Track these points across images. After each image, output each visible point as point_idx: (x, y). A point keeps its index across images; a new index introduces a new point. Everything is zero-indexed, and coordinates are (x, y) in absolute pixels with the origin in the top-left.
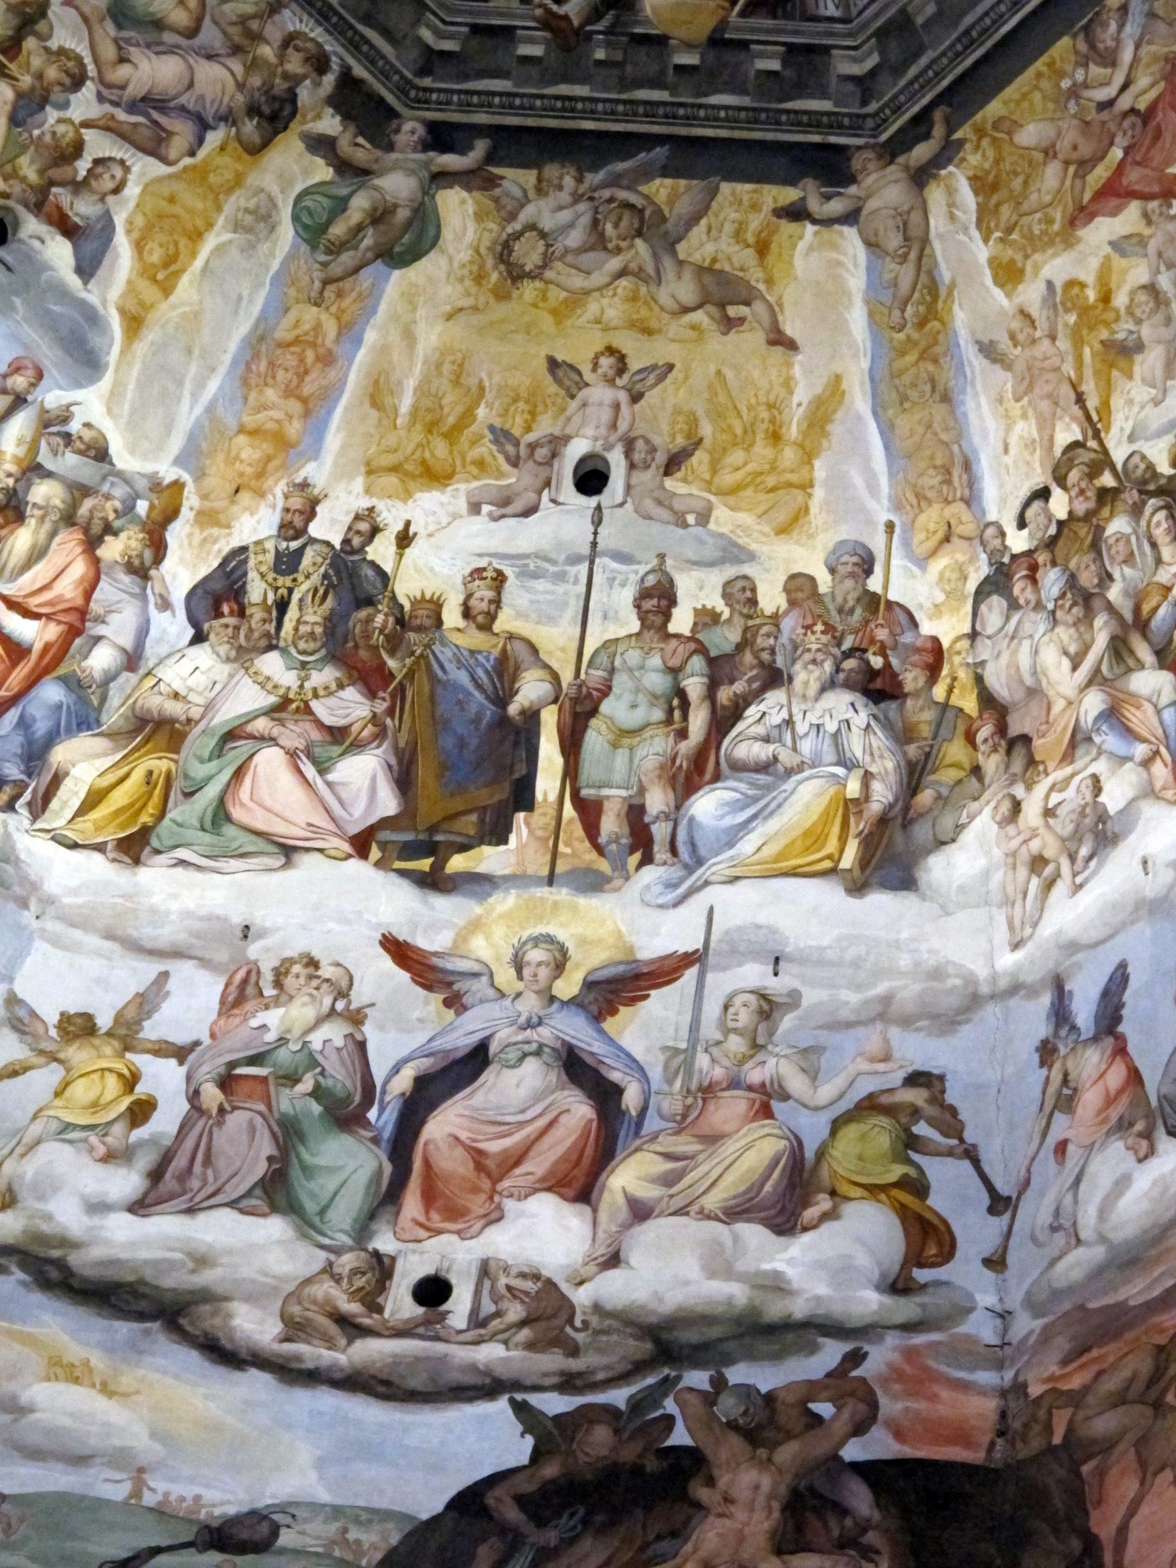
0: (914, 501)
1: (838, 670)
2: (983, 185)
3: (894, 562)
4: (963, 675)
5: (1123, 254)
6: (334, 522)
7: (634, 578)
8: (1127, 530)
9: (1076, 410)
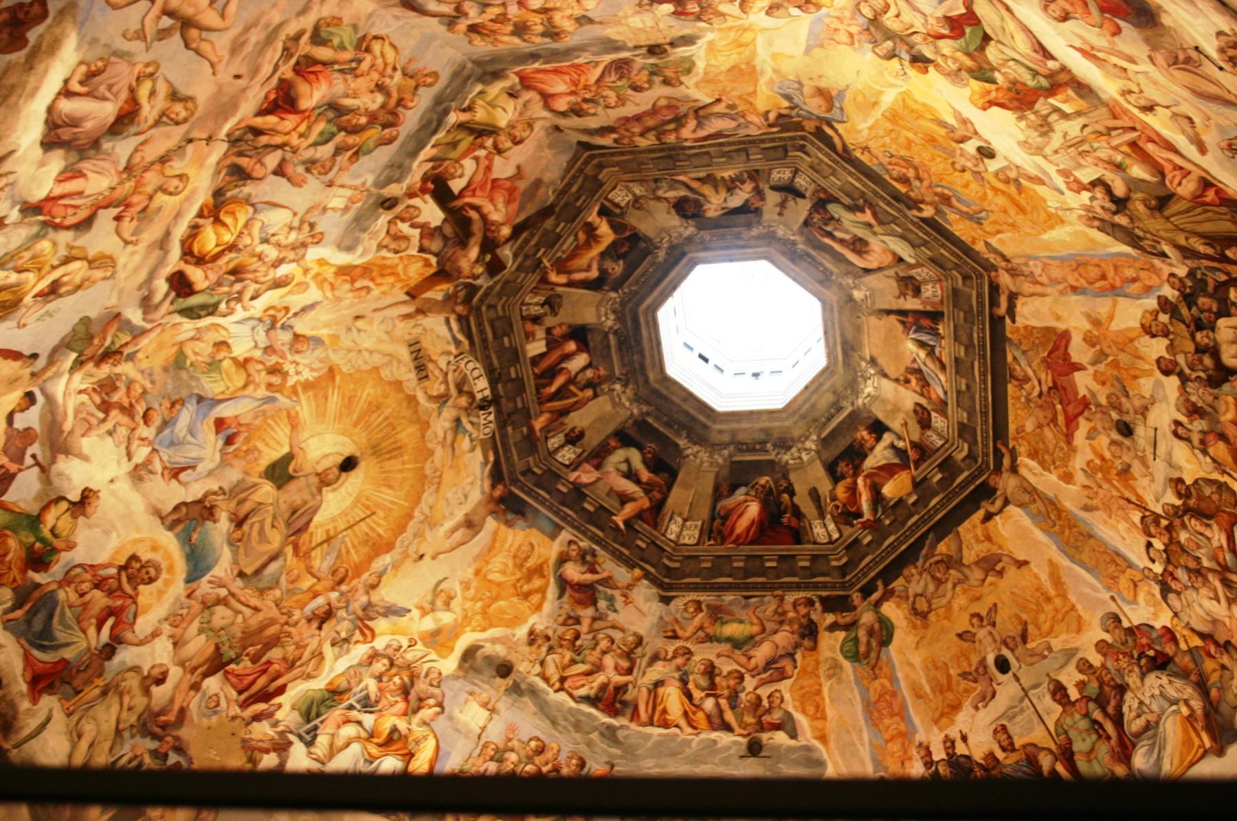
1: (1141, 667)
2: (1033, 455)
3: (1126, 609)
4: (1186, 632)
5: (1093, 439)
7: (1045, 690)
8: (1187, 535)
9: (1132, 506)
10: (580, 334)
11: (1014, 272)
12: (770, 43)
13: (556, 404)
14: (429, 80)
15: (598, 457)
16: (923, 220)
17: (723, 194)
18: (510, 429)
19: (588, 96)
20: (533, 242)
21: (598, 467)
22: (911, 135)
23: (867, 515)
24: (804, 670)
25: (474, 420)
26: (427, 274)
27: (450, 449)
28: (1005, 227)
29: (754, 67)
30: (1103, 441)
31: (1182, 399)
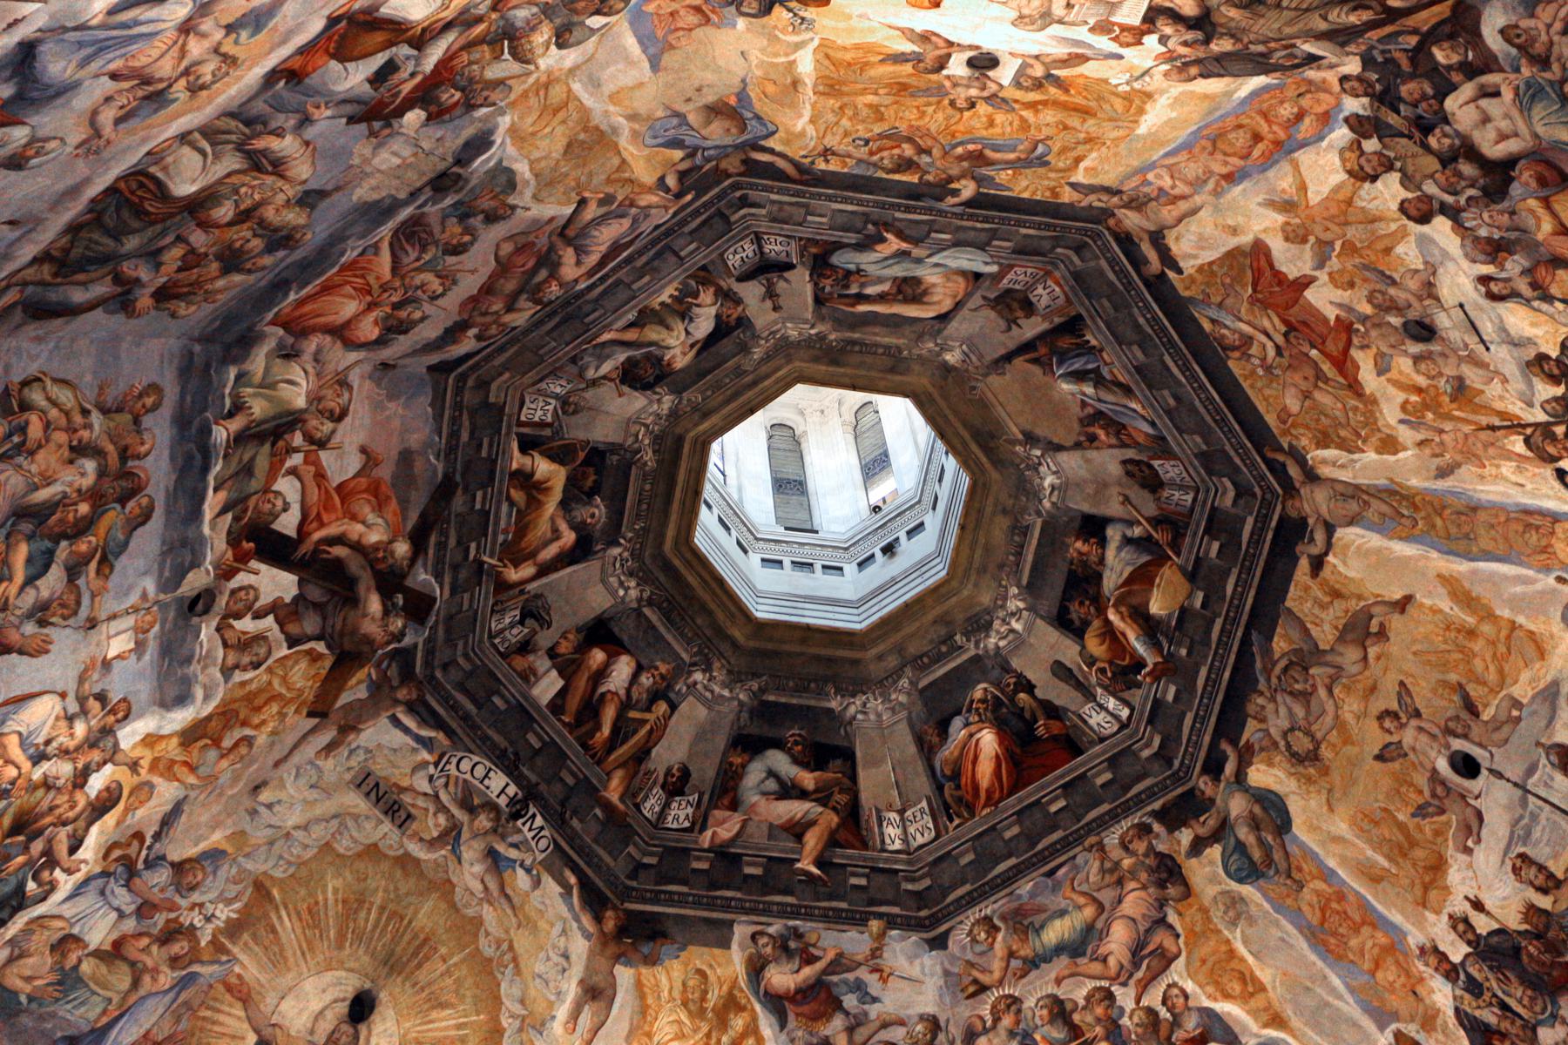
0: (1544, 556)
5: (1388, 370)
6: (1452, 943)
7: (1549, 769)
9: (1499, 433)
10: (600, 633)
11: (1137, 203)
12: (595, 84)
13: (623, 751)
14: (149, 401)
15: (726, 791)
16: (968, 203)
17: (679, 327)
18: (575, 823)
19: (394, 299)
20: (452, 542)
21: (734, 806)
22: (870, 98)
23: (1151, 659)
24: (1191, 932)
25: (515, 838)
26: (324, 672)
27: (503, 900)
28: (1081, 149)
29: (597, 128)
30: (1403, 365)
31: (1468, 242)
